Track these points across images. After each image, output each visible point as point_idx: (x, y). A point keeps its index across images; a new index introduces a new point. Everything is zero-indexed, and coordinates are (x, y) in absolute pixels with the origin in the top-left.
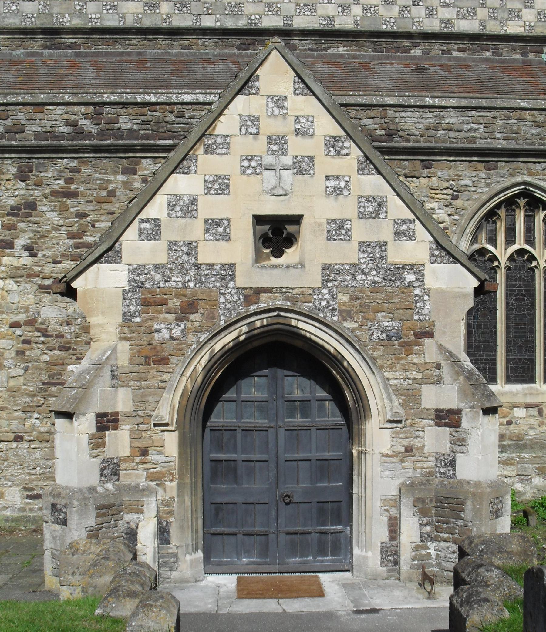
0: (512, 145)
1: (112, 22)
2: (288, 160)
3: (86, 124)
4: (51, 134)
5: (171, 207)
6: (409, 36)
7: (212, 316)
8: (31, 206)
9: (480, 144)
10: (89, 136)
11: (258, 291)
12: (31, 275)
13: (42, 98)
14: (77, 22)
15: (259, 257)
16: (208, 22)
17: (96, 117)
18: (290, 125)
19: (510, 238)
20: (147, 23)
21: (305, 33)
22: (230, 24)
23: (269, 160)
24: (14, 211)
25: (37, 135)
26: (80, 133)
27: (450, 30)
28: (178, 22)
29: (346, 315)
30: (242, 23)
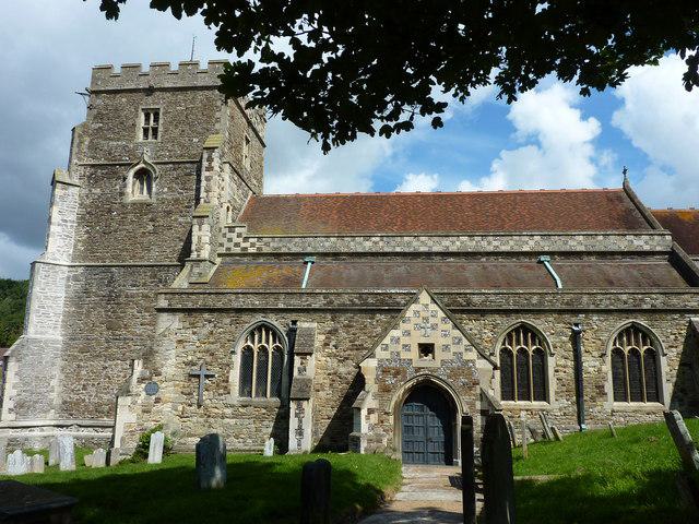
0: (517, 308)
1: (360, 250)
2: (429, 325)
3: (356, 301)
4: (344, 305)
5: (392, 340)
6: (480, 253)
7: (404, 376)
8: (336, 330)
9: (504, 307)
10: (357, 305)
11: (420, 368)
12: (335, 356)
13: (340, 291)
14: (346, 250)
15: (420, 357)
16: (398, 249)
17: (359, 299)
18: (429, 314)
19: (518, 343)
20: (374, 250)
21: (437, 254)
22: (407, 250)
23: (423, 325)
24: (330, 332)
25: (339, 305)
26: (354, 304)
27: (498, 250)
28: (387, 250)
29: (450, 377)
30: (412, 250)
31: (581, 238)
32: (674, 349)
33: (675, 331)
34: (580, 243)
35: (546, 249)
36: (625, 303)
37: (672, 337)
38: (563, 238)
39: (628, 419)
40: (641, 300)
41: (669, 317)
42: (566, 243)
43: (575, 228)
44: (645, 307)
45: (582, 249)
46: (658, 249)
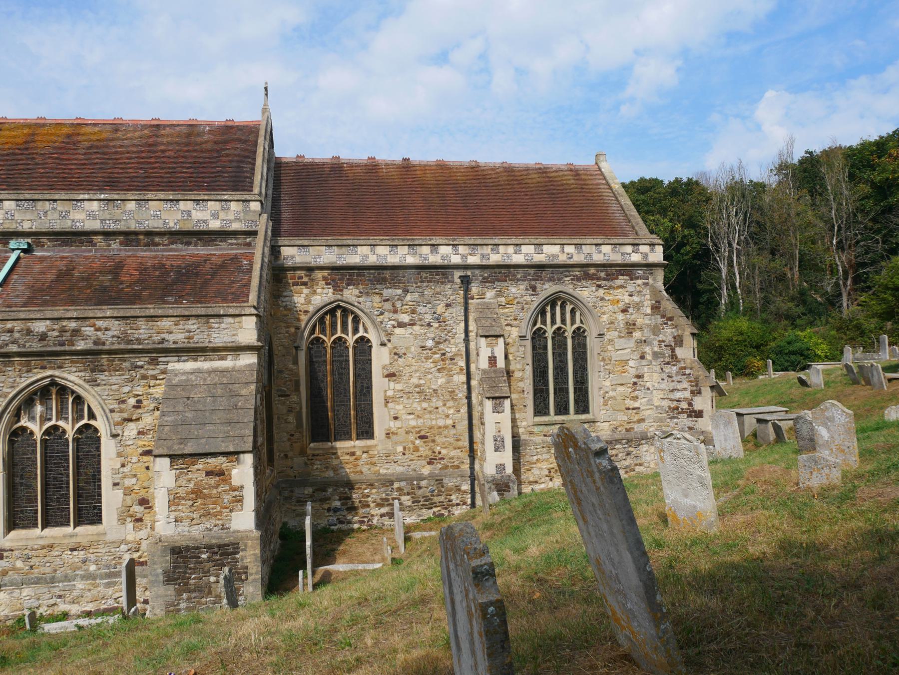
31: (95, 204)
32: (132, 425)
33: (139, 390)
34: (92, 216)
35: (26, 226)
36: (43, 337)
37: (132, 401)
38: (60, 206)
39: (33, 561)
40: (76, 332)
41: (126, 365)
42: (64, 215)
43: (87, 189)
44: (81, 346)
45: (96, 225)
46: (236, 226)
